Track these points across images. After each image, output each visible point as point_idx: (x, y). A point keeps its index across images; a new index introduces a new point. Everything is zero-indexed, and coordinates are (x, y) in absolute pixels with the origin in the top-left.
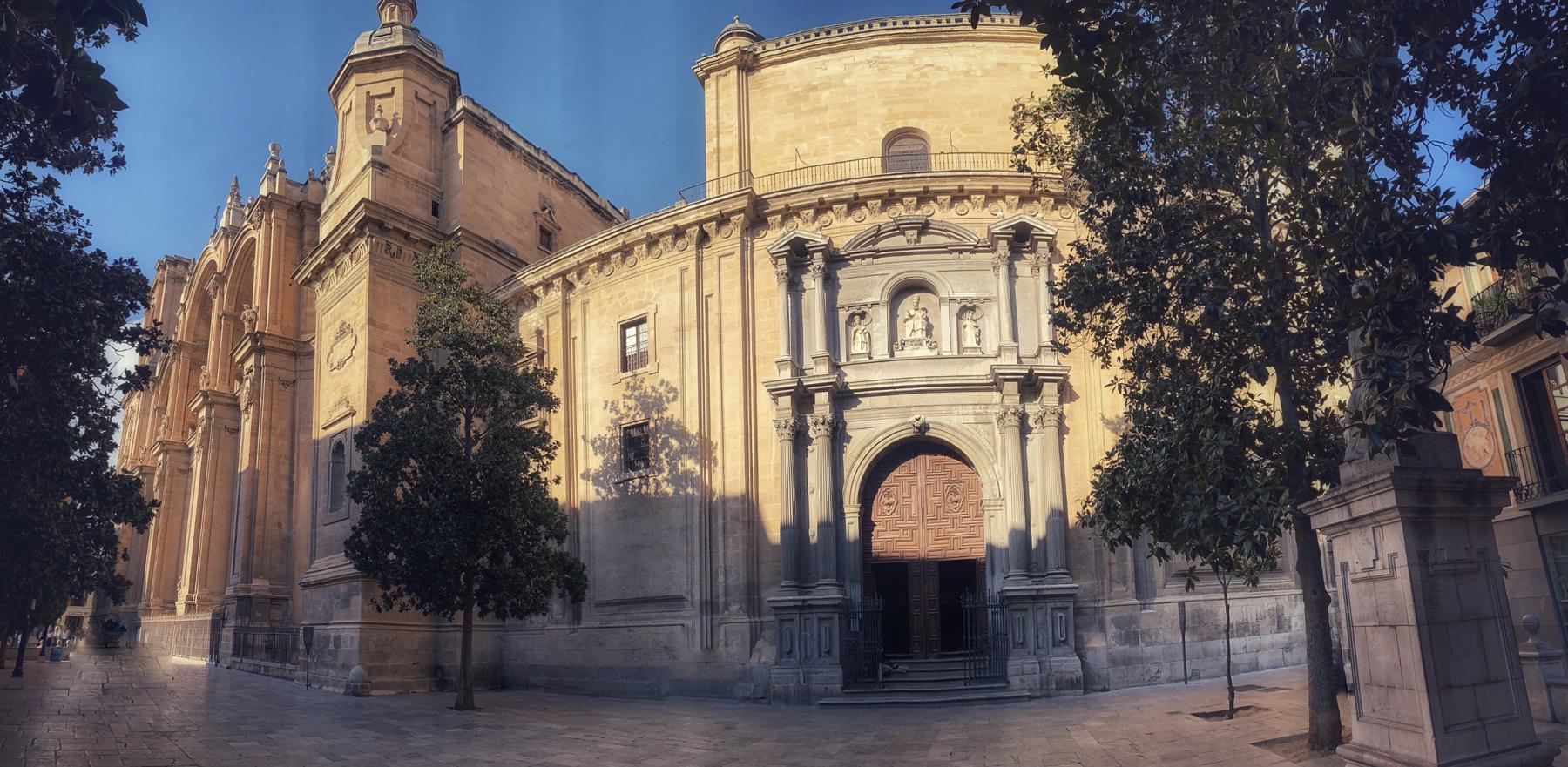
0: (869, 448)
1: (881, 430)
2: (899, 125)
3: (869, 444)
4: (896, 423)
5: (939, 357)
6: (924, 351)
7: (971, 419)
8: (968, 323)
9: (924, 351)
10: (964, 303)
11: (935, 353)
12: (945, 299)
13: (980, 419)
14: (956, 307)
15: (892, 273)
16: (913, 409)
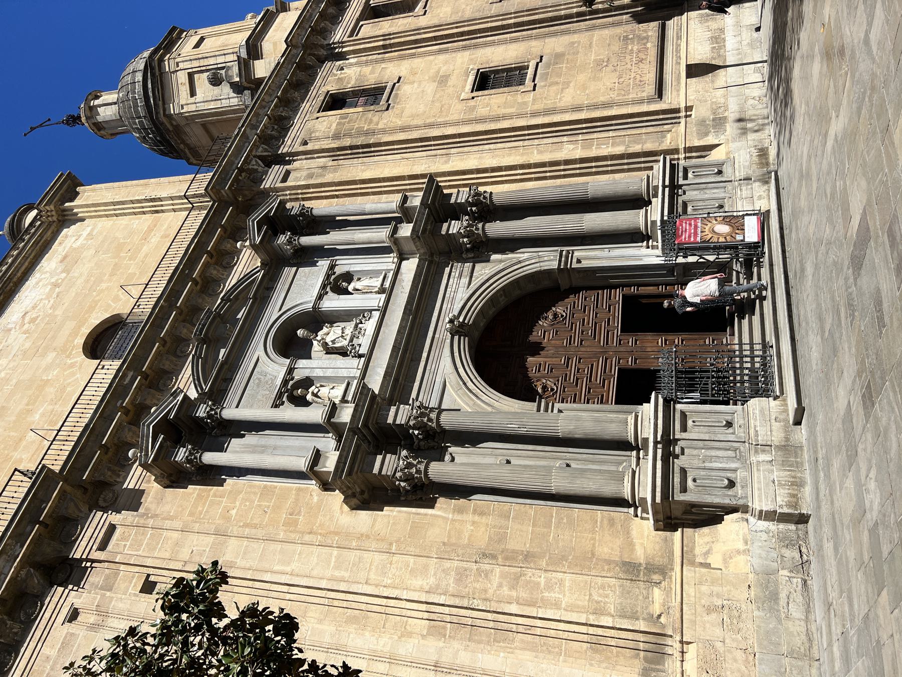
0: (470, 384)
1: (452, 369)
2: (80, 341)
3: (465, 384)
4: (449, 359)
5: (384, 311)
6: (370, 326)
7: (464, 280)
8: (350, 288)
9: (370, 326)
10: (328, 289)
11: (376, 315)
12: (315, 304)
13: (465, 273)
14: (331, 294)
15: (260, 352)
16: (437, 336)
